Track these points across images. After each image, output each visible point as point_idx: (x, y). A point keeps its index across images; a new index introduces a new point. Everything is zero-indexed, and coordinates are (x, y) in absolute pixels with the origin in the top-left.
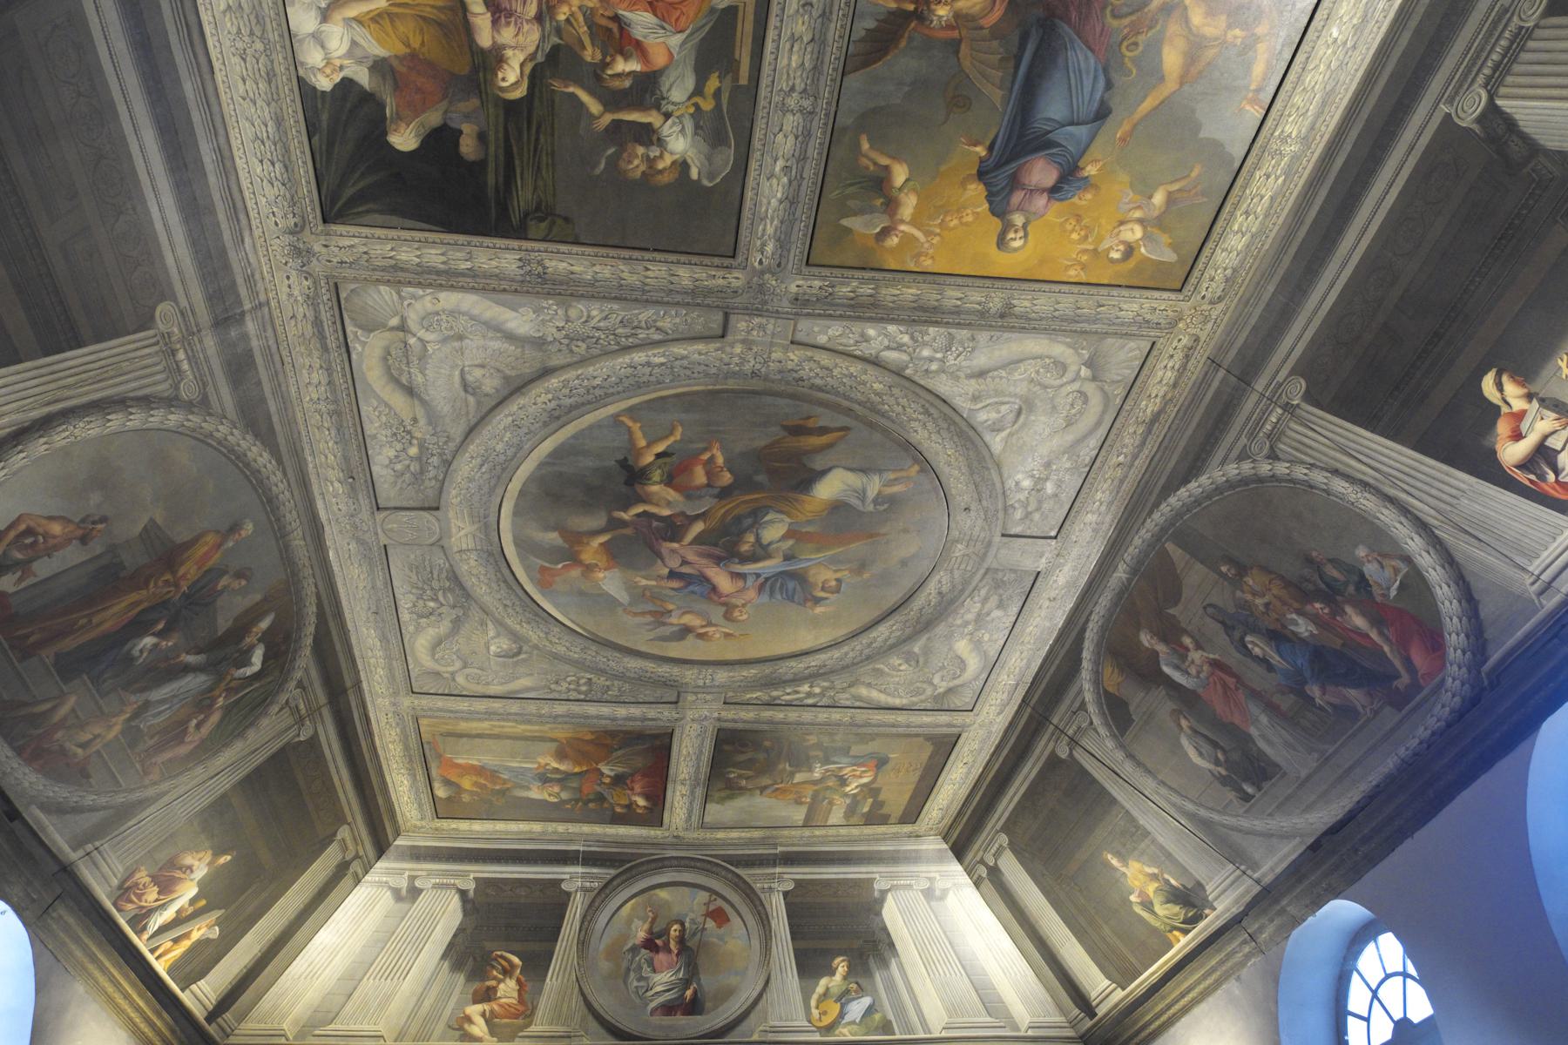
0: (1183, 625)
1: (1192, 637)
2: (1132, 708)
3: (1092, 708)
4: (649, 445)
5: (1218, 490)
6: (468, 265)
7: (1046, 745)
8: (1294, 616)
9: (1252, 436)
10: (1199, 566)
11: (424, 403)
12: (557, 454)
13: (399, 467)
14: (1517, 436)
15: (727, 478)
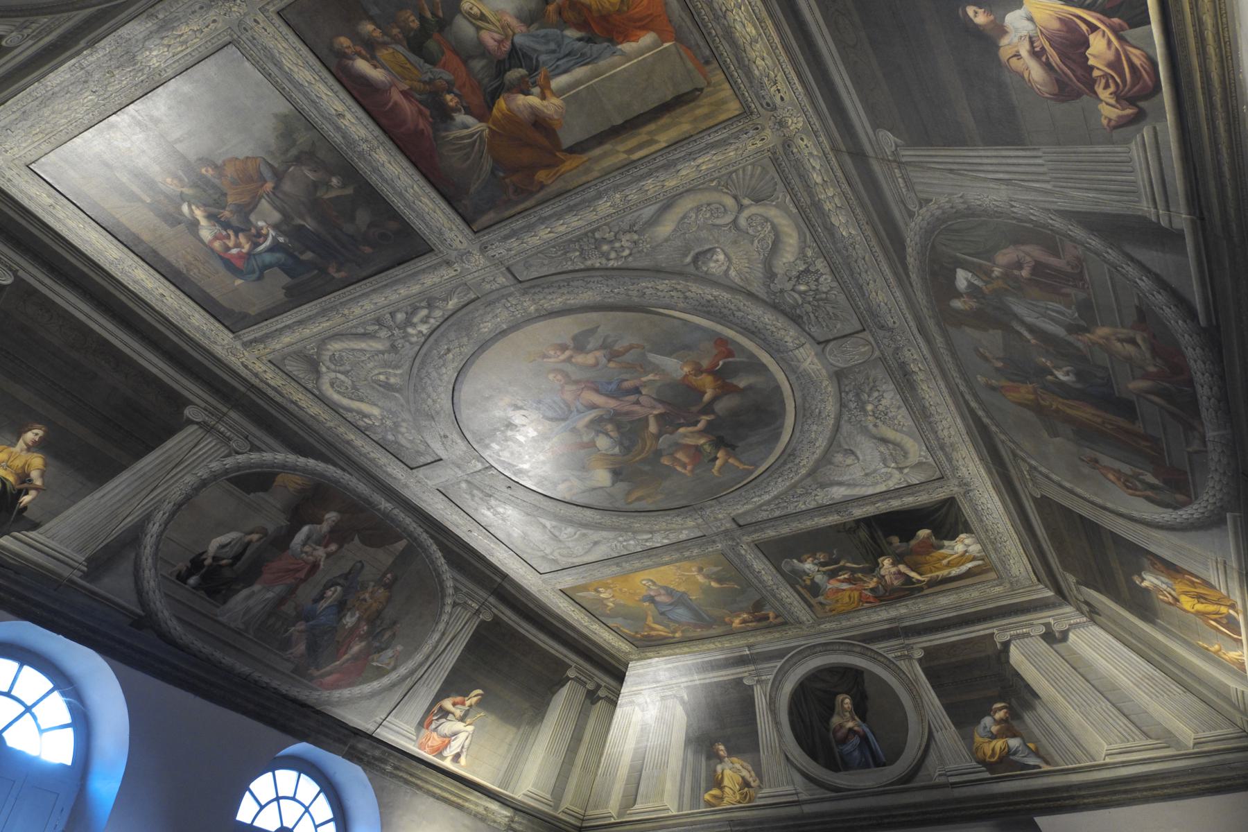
0: (346, 546)
1: (336, 552)
2: (261, 494)
3: (255, 457)
4: (726, 461)
5: (439, 575)
6: (877, 505)
7: (203, 400)
8: (357, 615)
9: (467, 595)
10: (391, 560)
11: (874, 437)
12: (777, 436)
13: (876, 394)
14: (454, 704)
15: (665, 461)
